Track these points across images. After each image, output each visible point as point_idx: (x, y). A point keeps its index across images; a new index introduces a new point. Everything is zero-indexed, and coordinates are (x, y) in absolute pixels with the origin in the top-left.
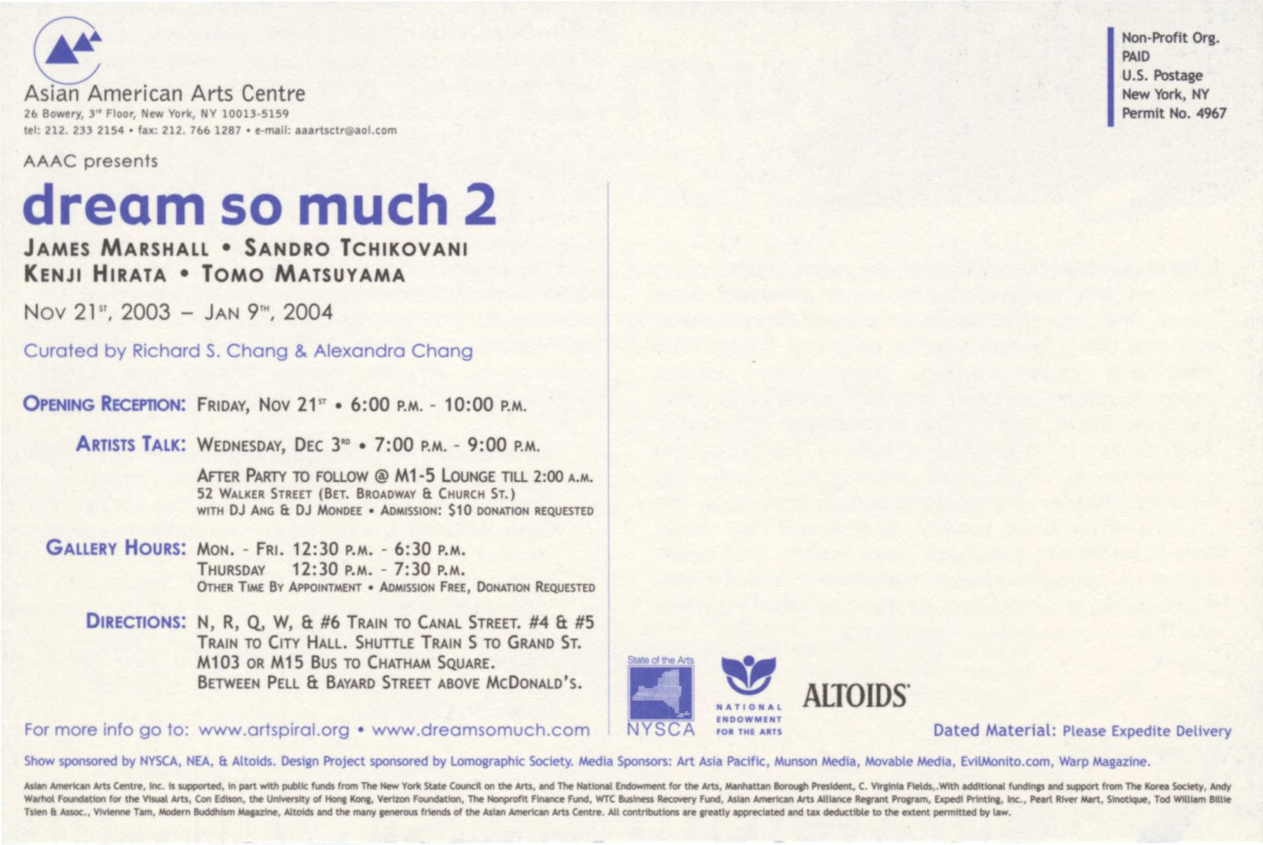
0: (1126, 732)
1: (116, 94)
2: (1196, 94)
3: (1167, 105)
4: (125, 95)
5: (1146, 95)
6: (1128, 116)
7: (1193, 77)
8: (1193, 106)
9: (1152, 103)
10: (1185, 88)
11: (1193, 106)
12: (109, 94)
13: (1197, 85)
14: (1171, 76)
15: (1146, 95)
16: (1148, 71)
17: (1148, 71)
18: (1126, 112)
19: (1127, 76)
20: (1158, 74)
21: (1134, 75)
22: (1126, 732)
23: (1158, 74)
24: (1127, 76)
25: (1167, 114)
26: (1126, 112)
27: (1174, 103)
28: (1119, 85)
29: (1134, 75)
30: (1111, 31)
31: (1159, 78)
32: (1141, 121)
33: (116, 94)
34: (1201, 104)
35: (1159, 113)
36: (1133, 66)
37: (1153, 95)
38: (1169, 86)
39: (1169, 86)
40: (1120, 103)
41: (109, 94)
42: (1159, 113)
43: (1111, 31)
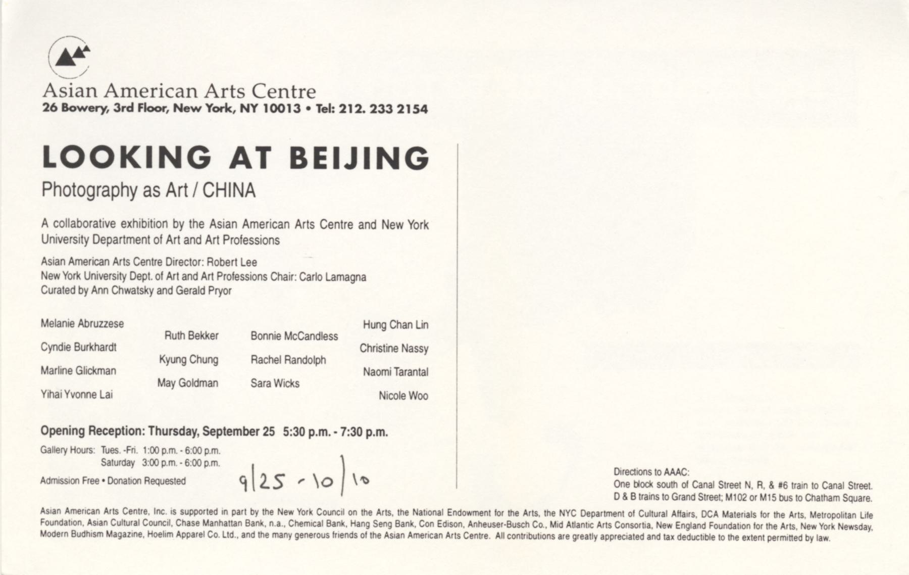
1: (132, 92)
12: (126, 92)
33: (132, 92)
41: (126, 92)
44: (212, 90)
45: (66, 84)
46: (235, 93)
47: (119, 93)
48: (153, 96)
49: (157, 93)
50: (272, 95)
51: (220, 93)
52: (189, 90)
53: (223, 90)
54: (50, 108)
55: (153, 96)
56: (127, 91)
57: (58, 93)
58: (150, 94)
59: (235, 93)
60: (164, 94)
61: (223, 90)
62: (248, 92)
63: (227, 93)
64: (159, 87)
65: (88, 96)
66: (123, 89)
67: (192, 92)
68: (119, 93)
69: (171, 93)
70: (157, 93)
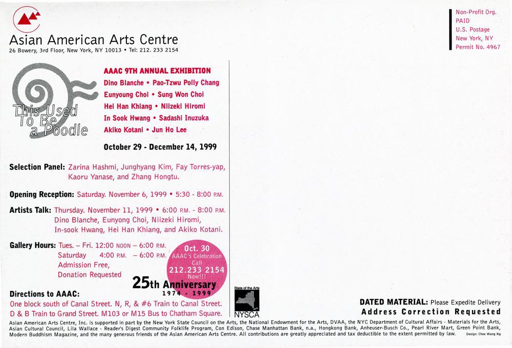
0: (458, 303)
2: (487, 38)
3: (474, 43)
5: (465, 39)
7: (488, 30)
9: (468, 42)
10: (482, 35)
11: (485, 43)
13: (487, 34)
15: (465, 39)
16: (467, 29)
17: (467, 29)
18: (457, 46)
19: (458, 30)
20: (471, 29)
21: (461, 29)
22: (458, 303)
23: (471, 29)
24: (458, 30)
25: (475, 47)
26: (457, 46)
29: (461, 29)
30: (450, 11)
31: (472, 31)
32: (464, 50)
34: (490, 42)
35: (471, 47)
36: (461, 25)
37: (469, 39)
38: (476, 34)
39: (476, 34)
42: (471, 47)
43: (450, 11)
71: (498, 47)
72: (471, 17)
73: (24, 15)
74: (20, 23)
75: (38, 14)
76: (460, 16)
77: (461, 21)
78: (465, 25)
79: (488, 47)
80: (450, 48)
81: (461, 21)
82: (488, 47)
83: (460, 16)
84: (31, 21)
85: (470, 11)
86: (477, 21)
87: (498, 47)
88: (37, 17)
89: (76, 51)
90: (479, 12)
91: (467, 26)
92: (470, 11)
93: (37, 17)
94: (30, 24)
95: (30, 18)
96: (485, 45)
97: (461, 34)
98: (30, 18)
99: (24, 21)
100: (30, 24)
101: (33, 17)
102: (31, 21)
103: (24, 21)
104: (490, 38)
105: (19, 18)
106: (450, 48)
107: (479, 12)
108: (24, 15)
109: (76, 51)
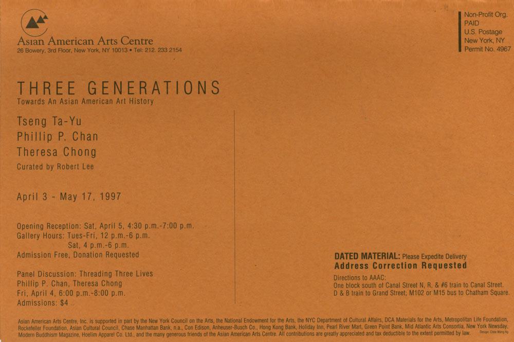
3: (484, 45)
4: (66, 43)
5: (476, 41)
6: (467, 50)
8: (495, 45)
9: (478, 45)
10: (493, 37)
11: (495, 45)
12: (59, 41)
13: (499, 36)
14: (487, 32)
15: (476, 41)
17: (477, 31)
19: (467, 32)
25: (484, 49)
26: (466, 48)
27: (489, 45)
28: (463, 36)
29: (470, 32)
30: (460, 13)
34: (500, 44)
35: (481, 49)
36: (471, 27)
38: (487, 37)
39: (487, 37)
40: (463, 44)
41: (59, 41)
42: (481, 49)
43: (460, 13)
44: (101, 40)
45: (30, 38)
46: (113, 42)
47: (56, 43)
48: (72, 44)
49: (74, 42)
50: (131, 43)
51: (106, 43)
52: (89, 40)
53: (107, 40)
54: (21, 50)
55: (72, 44)
56: (60, 42)
57: (25, 43)
58: (70, 43)
59: (113, 42)
60: (77, 43)
61: (107, 40)
62: (119, 42)
63: (109, 42)
64: (75, 39)
65: (40, 44)
66: (58, 40)
67: (91, 42)
68: (56, 43)
69: (80, 42)
70: (74, 42)
71: (508, 48)
72: (481, 18)
73: (32, 19)
74: (27, 27)
75: (46, 17)
76: (469, 19)
77: (470, 23)
78: (474, 27)
79: (499, 49)
80: (460, 50)
81: (470, 23)
82: (499, 49)
83: (469, 19)
84: (38, 24)
85: (480, 14)
86: (487, 24)
87: (508, 48)
88: (45, 20)
89: (84, 51)
90: (490, 14)
91: (476, 29)
92: (480, 14)
93: (45, 20)
94: (37, 27)
95: (38, 22)
96: (495, 49)
97: (470, 36)
98: (38, 22)
99: (32, 24)
100: (37, 27)
101: (41, 20)
102: (38, 24)
103: (32, 24)
104: (501, 41)
105: (26, 22)
106: (460, 50)
107: (490, 14)
108: (32, 19)
109: (84, 51)
